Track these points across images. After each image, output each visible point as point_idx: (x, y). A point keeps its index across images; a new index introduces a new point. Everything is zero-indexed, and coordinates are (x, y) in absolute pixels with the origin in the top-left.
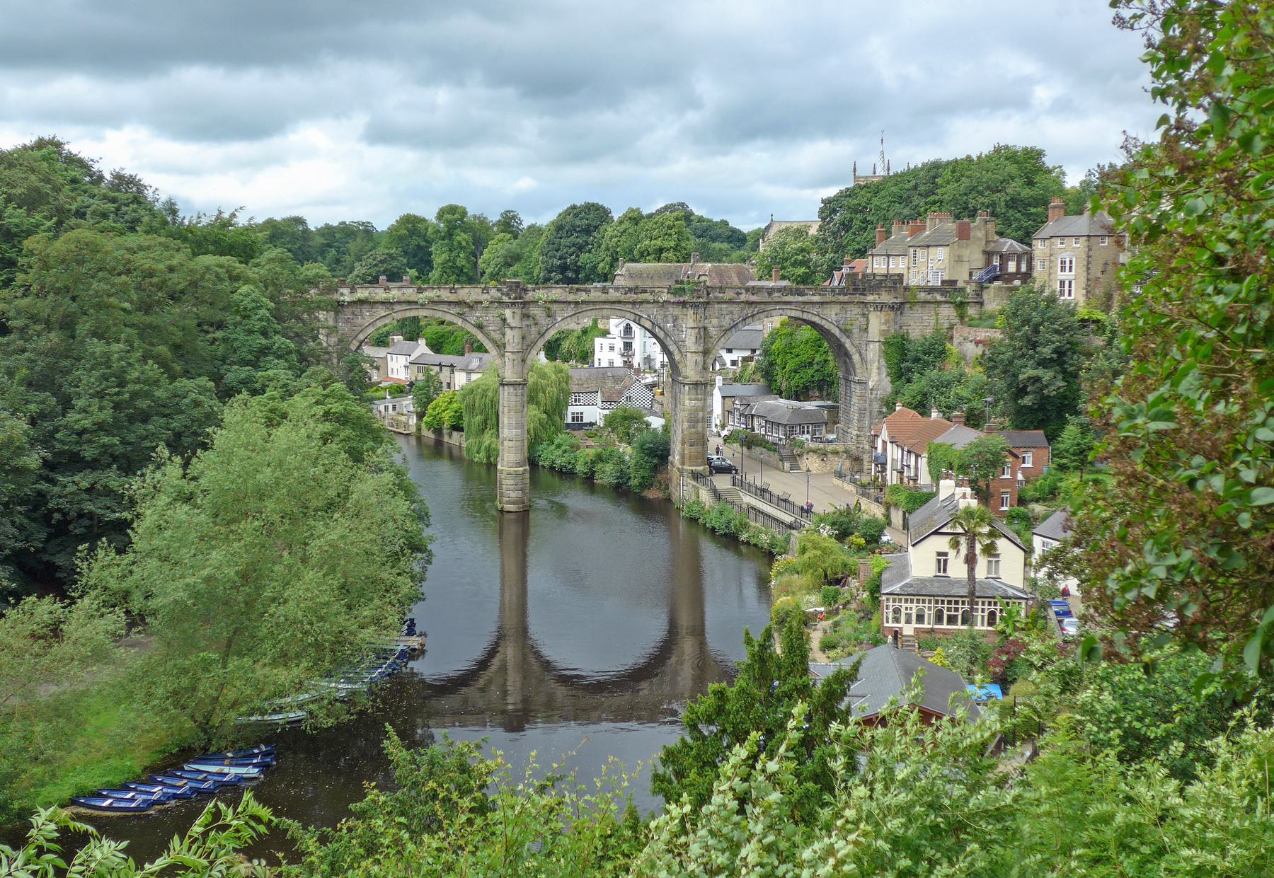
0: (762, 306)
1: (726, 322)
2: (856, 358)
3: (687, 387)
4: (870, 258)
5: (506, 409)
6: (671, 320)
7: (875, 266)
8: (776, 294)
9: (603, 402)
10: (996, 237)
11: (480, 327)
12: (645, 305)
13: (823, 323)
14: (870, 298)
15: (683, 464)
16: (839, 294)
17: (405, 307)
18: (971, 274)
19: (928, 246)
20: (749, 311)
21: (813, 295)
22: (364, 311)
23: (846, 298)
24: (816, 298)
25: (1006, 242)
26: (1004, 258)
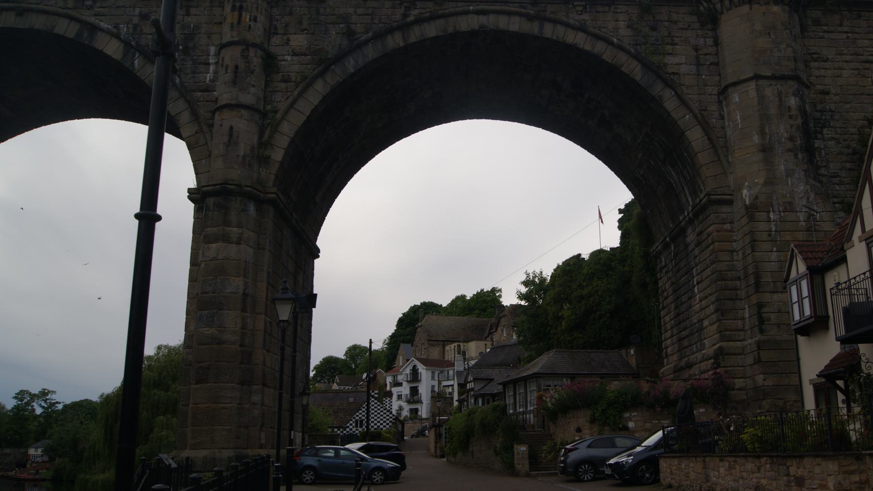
13: (599, 47)
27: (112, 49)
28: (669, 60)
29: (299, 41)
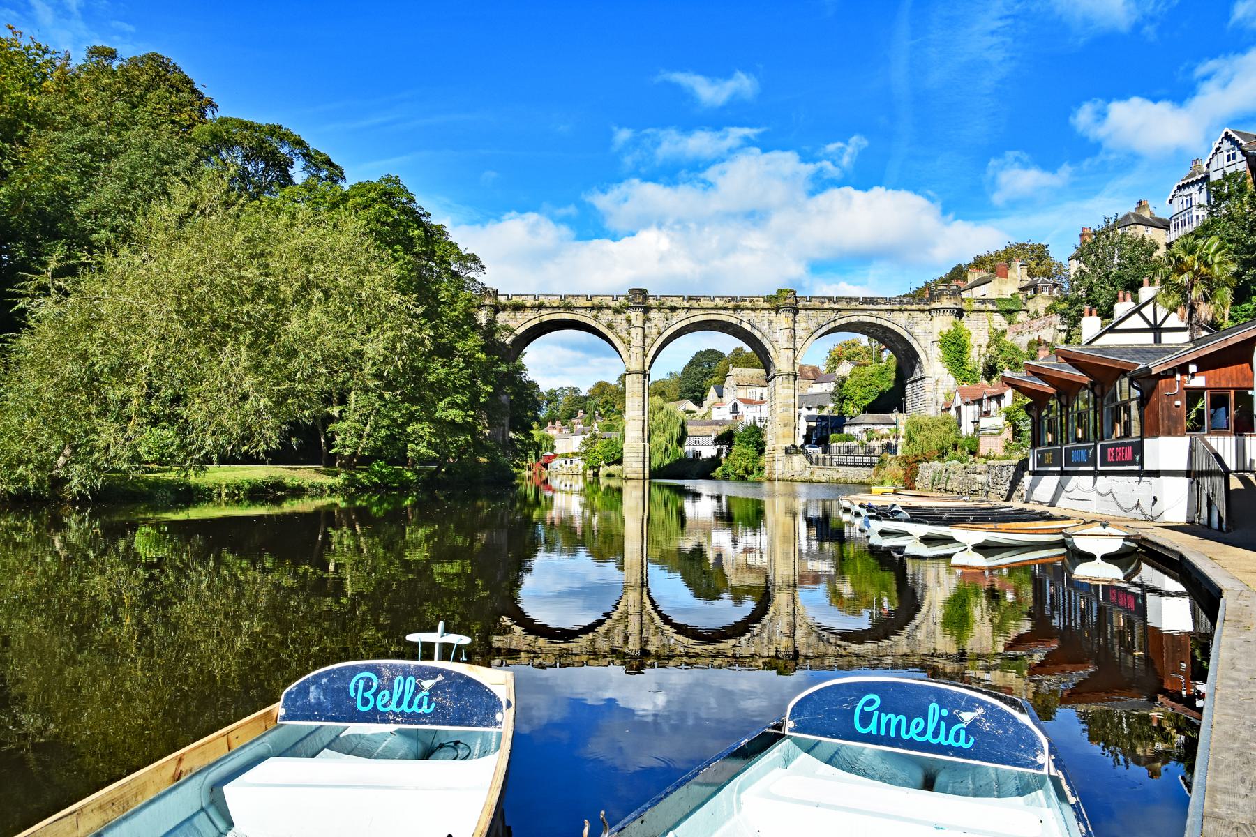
1: (813, 325)
2: (922, 356)
8: (853, 303)
11: (610, 327)
14: (934, 305)
17: (550, 311)
20: (831, 315)
23: (913, 307)
27: (747, 327)
29: (804, 325)
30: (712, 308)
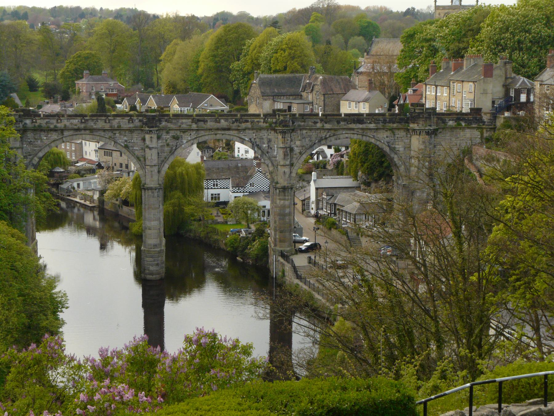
0: (333, 132)
1: (307, 142)
2: (402, 168)
3: (278, 191)
4: (424, 86)
5: (147, 207)
6: (265, 141)
7: (428, 93)
8: (342, 123)
9: (233, 187)
10: (513, 75)
12: (247, 131)
13: (378, 143)
14: (412, 125)
15: (275, 245)
16: (389, 122)
17: (71, 133)
18: (493, 102)
19: (463, 81)
20: (323, 134)
21: (370, 123)
22: (42, 136)
23: (395, 125)
24: (372, 126)
25: (520, 79)
26: (518, 93)
28: (397, 146)
30: (218, 129)
